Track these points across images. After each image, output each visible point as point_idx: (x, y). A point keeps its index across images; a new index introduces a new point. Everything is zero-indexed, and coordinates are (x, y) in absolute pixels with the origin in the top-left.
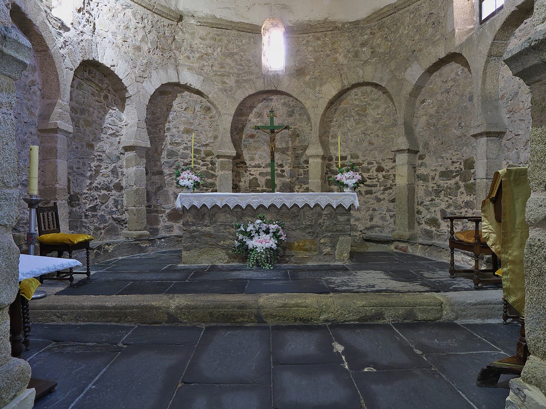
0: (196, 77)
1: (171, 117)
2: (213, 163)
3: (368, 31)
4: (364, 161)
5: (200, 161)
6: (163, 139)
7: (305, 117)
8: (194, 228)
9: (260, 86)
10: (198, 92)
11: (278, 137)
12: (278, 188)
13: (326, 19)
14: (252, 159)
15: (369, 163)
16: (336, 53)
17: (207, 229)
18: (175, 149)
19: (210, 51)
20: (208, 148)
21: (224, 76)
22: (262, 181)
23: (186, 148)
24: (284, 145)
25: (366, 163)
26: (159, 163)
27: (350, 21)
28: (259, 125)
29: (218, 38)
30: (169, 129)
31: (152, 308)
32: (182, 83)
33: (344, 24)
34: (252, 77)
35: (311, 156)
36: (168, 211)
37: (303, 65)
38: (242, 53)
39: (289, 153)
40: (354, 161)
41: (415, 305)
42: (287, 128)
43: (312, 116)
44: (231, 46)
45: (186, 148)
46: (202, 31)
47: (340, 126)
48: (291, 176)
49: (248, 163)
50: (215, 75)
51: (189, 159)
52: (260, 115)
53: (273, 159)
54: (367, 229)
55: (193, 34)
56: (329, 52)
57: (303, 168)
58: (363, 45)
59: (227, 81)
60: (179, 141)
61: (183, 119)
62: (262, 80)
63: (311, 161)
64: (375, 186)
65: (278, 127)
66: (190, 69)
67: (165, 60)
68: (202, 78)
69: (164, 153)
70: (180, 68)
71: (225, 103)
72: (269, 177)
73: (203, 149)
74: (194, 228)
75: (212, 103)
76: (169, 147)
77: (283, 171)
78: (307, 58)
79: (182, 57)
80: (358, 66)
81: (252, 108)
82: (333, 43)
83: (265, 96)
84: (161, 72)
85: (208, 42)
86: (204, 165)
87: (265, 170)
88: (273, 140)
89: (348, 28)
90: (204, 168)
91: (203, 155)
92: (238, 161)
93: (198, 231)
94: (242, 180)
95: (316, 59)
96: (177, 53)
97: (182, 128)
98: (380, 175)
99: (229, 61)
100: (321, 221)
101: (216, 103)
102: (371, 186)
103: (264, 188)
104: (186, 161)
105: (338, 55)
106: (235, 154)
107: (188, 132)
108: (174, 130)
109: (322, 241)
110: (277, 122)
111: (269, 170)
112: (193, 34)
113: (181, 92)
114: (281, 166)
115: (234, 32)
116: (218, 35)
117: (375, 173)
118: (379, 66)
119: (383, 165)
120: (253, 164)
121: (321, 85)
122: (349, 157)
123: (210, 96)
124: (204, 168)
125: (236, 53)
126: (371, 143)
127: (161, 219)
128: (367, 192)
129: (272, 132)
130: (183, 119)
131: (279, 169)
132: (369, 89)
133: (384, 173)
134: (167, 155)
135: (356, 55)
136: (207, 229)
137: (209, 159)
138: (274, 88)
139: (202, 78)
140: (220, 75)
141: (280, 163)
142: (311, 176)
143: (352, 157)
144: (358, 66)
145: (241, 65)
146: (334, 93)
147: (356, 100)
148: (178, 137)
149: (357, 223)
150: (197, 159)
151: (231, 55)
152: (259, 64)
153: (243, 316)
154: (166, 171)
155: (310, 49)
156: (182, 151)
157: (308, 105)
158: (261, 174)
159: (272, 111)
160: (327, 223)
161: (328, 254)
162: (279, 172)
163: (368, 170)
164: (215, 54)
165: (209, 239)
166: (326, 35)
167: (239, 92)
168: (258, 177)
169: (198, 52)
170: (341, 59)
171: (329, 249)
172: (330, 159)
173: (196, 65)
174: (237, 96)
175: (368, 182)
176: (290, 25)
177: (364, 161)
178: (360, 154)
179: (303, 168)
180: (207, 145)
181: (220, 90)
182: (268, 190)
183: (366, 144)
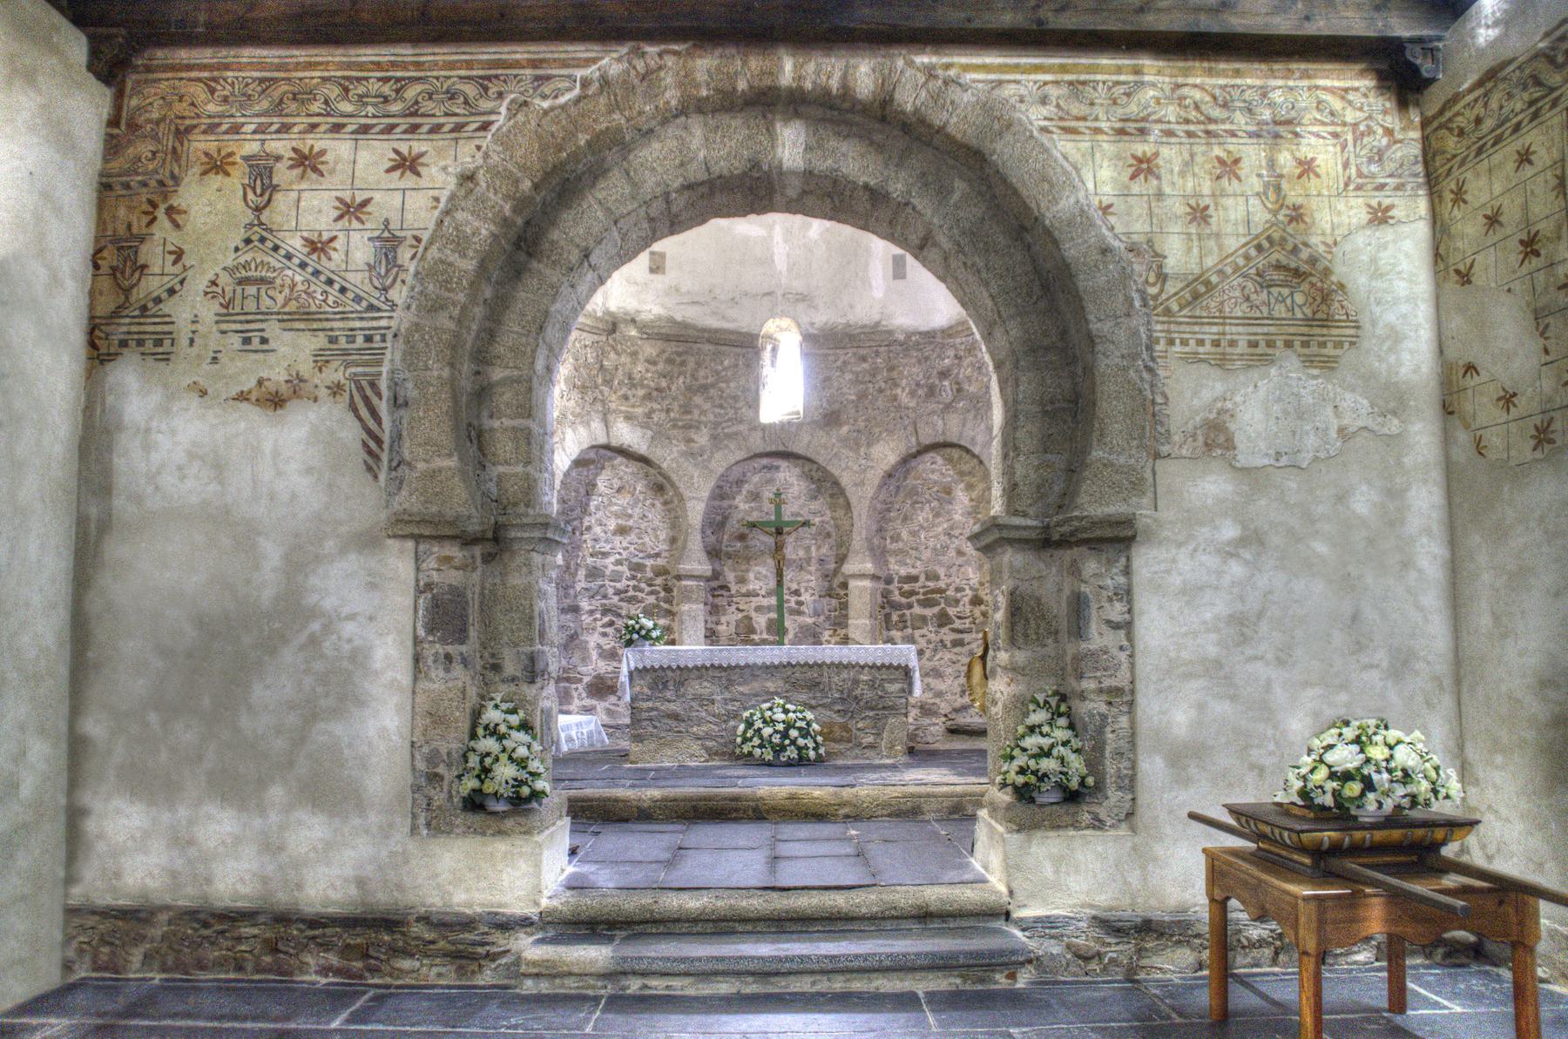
0: (639, 432)
1: (593, 504)
2: (668, 589)
3: (951, 353)
4: (948, 585)
5: (643, 585)
6: (579, 548)
7: (841, 500)
8: (650, 704)
9: (757, 443)
10: (644, 460)
11: (790, 540)
12: (790, 635)
13: (877, 324)
14: (742, 580)
15: (958, 590)
16: (896, 385)
17: (672, 706)
18: (599, 562)
19: (664, 384)
20: (660, 562)
21: (690, 427)
22: (761, 621)
23: (619, 563)
24: (801, 553)
25: (952, 588)
26: (572, 592)
27: (922, 329)
28: (755, 517)
29: (678, 359)
30: (589, 528)
31: (616, 800)
32: (614, 443)
33: (909, 335)
34: (741, 427)
35: (854, 576)
36: (586, 680)
37: (836, 406)
38: (723, 385)
39: (812, 568)
40: (931, 584)
41: (964, 795)
42: (806, 524)
43: (853, 501)
44: (702, 373)
45: (619, 563)
46: (649, 350)
47: (905, 519)
48: (816, 614)
49: (734, 588)
50: (674, 426)
51: (625, 582)
52: (755, 496)
53: (780, 583)
54: (956, 710)
55: (634, 354)
56: (883, 385)
57: (838, 597)
58: (944, 374)
59: (695, 437)
60: (607, 548)
61: (615, 508)
62: (760, 434)
63: (853, 583)
64: (969, 631)
65: (788, 524)
66: (628, 417)
67: (588, 407)
68: (650, 433)
69: (582, 573)
70: (611, 418)
71: (692, 477)
72: (774, 615)
73: (649, 562)
74: (650, 704)
75: (667, 478)
76: (590, 560)
77: (800, 603)
78: (843, 394)
79: (614, 398)
80: (934, 412)
81: (740, 483)
82: (891, 369)
83: (765, 461)
84: (582, 430)
85: (660, 367)
86: (652, 593)
87: (765, 602)
88: (779, 548)
89: (918, 344)
90: (651, 599)
91: (650, 574)
92: (715, 584)
93: (656, 709)
94: (723, 619)
95: (862, 396)
96: (606, 389)
97: (612, 524)
98: (977, 612)
99: (698, 400)
100: (858, 692)
101: (674, 477)
102: (961, 632)
103: (765, 636)
104: (618, 585)
105: (899, 391)
106: (709, 573)
107: (622, 531)
108: (598, 530)
109: (860, 725)
110: (788, 513)
111: (773, 601)
112: (634, 354)
113: (610, 459)
114: (797, 593)
115: (707, 347)
116: (679, 354)
117: (968, 608)
118: (970, 416)
119: (982, 594)
120: (744, 590)
121: (869, 445)
122: (922, 578)
123: (665, 465)
124: (651, 599)
125: (712, 385)
126: (960, 553)
127: (575, 694)
128: (956, 643)
129: (779, 532)
130: (615, 508)
131: (794, 599)
132: (955, 453)
133: (983, 607)
134: (587, 576)
135: (932, 392)
136: (672, 706)
137: (659, 581)
138: (781, 448)
139: (650, 433)
140: (683, 427)
141: (794, 586)
142: (851, 613)
143: (928, 578)
144: (934, 412)
145: (721, 406)
146: (892, 459)
147: (933, 472)
148: (607, 541)
149: (937, 701)
150: (639, 581)
151: (704, 388)
152: (754, 404)
153: (737, 810)
154: (585, 605)
155: (848, 376)
156: (611, 567)
157: (846, 480)
158: (758, 609)
159: (778, 494)
160: (868, 694)
161: (871, 747)
162: (793, 604)
163: (957, 601)
164: (673, 388)
165: (674, 723)
166: (877, 354)
167: (718, 455)
168: (753, 614)
169: (643, 386)
170: (904, 398)
171: (871, 739)
172: (889, 581)
173: (639, 411)
174: (713, 464)
175: (958, 624)
176: (812, 331)
177: (948, 585)
178: (942, 572)
179: (838, 597)
180: (657, 555)
181: (683, 454)
182: (771, 638)
183: (953, 553)
